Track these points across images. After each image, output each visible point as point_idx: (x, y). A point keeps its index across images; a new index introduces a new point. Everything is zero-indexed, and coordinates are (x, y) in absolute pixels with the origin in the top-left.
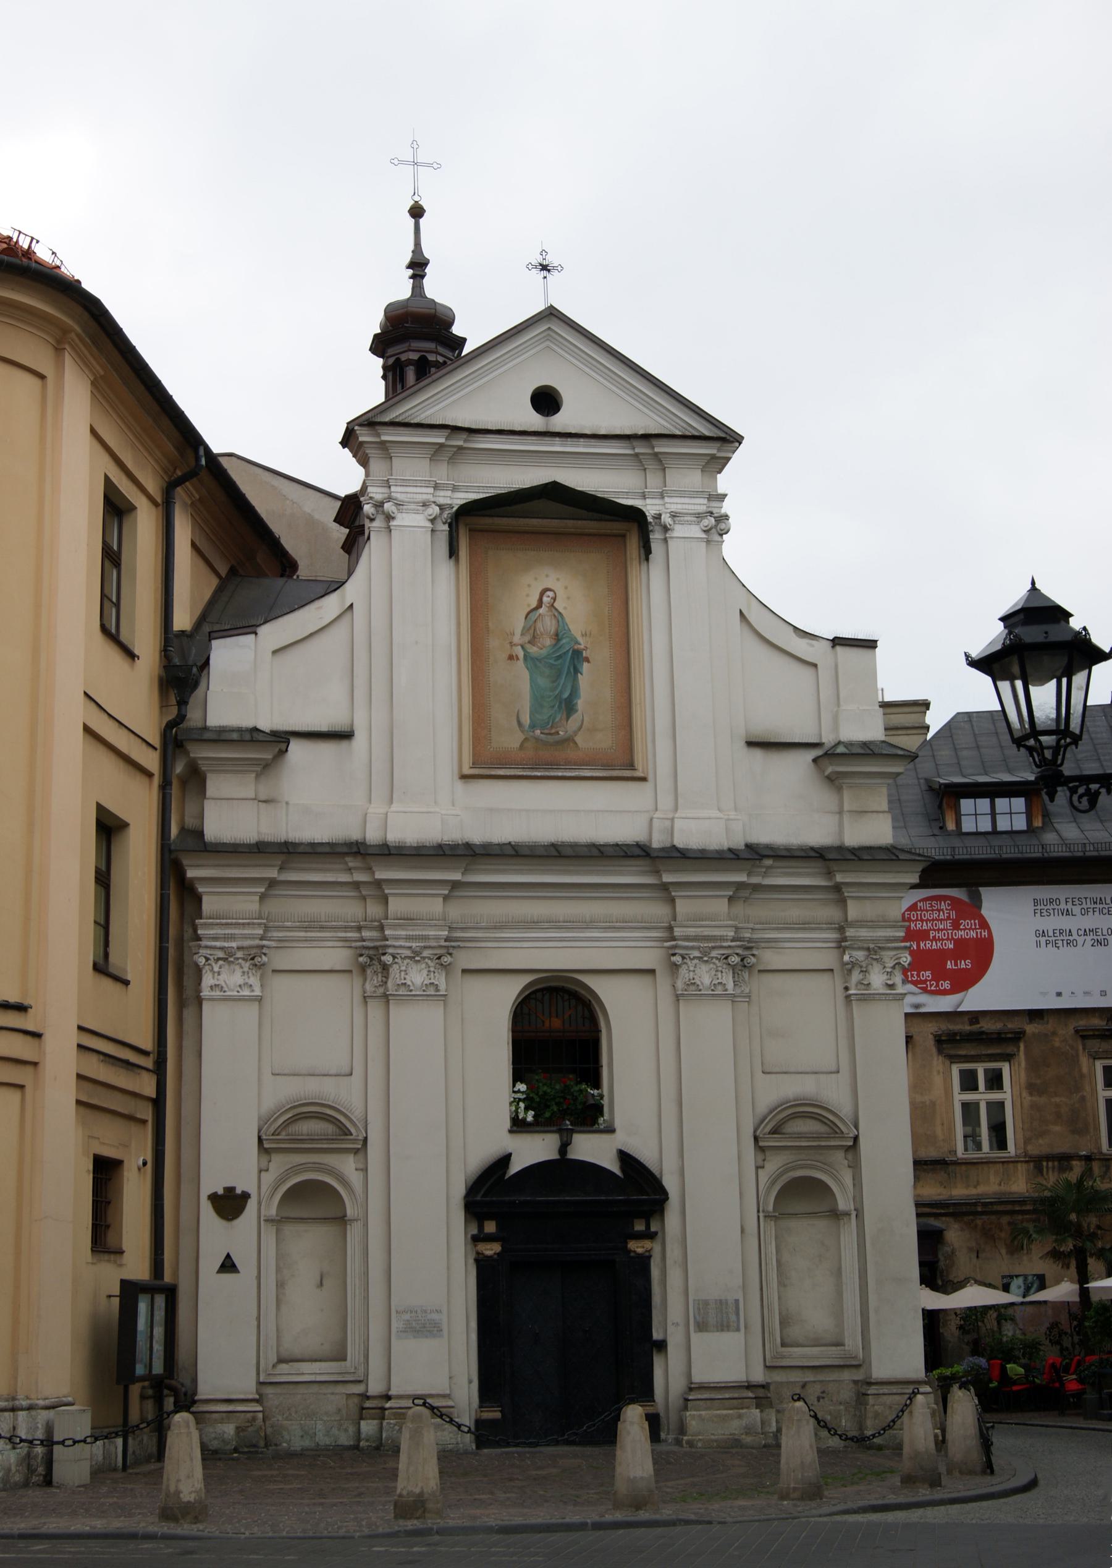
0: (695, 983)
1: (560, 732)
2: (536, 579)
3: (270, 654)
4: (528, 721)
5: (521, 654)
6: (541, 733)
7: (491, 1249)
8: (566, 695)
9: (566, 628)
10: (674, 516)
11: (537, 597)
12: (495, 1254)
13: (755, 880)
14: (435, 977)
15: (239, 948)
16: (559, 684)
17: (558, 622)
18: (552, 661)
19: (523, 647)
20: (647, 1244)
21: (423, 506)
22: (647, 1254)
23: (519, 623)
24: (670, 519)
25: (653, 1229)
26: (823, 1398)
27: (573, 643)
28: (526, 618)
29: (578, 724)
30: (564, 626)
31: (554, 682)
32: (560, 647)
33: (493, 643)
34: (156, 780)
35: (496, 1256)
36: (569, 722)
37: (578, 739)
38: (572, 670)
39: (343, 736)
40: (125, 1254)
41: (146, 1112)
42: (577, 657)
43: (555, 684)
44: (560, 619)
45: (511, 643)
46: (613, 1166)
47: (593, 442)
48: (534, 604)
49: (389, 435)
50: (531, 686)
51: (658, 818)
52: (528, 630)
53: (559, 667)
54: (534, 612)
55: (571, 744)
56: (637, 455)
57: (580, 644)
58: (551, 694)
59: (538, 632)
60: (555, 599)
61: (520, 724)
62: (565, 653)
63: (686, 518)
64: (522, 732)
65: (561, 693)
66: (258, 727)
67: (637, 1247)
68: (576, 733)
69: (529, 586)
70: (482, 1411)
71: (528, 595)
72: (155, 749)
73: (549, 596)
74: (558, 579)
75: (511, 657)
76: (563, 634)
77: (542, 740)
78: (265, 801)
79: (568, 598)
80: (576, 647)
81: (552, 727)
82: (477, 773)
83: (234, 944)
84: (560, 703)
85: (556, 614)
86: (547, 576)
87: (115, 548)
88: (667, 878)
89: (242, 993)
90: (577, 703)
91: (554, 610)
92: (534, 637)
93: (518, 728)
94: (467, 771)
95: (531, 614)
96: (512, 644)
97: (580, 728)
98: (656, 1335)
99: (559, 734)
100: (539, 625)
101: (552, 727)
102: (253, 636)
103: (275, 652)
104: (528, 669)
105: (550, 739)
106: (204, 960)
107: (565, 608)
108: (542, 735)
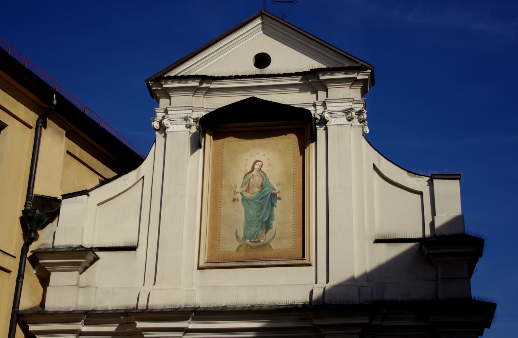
1: (261, 241)
2: (251, 156)
3: (96, 205)
4: (242, 235)
5: (240, 197)
6: (250, 242)
9: (268, 182)
10: (331, 113)
11: (251, 165)
13: (376, 323)
16: (262, 213)
17: (263, 178)
18: (258, 201)
19: (241, 193)
21: (185, 120)
23: (240, 180)
24: (328, 115)
27: (271, 190)
28: (244, 177)
29: (272, 236)
30: (266, 181)
31: (259, 212)
32: (264, 192)
33: (224, 192)
36: (267, 234)
37: (271, 244)
38: (270, 205)
39: (133, 248)
42: (274, 197)
43: (260, 213)
44: (264, 177)
45: (234, 192)
47: (284, 78)
48: (249, 169)
49: (167, 85)
50: (245, 215)
51: (317, 287)
52: (245, 184)
53: (263, 203)
54: (249, 174)
55: (268, 247)
56: (310, 84)
57: (275, 190)
58: (257, 219)
59: (251, 185)
60: (262, 166)
61: (237, 237)
62: (266, 196)
63: (338, 114)
64: (238, 241)
65: (263, 218)
66: (84, 246)
68: (271, 240)
69: (247, 160)
71: (246, 165)
72: (15, 257)
73: (258, 165)
74: (264, 155)
75: (234, 200)
76: (266, 185)
77: (250, 246)
78: (84, 287)
79: (270, 165)
80: (273, 192)
81: (256, 238)
82: (208, 266)
84: (262, 224)
85: (262, 174)
86: (258, 154)
90: (272, 224)
91: (261, 172)
92: (248, 188)
93: (236, 240)
94: (202, 264)
95: (247, 176)
96: (235, 193)
97: (273, 238)
99: (260, 242)
100: (252, 181)
101: (256, 238)
102: (86, 196)
103: (99, 205)
104: (244, 206)
105: (255, 245)
107: (268, 171)
108: (250, 243)
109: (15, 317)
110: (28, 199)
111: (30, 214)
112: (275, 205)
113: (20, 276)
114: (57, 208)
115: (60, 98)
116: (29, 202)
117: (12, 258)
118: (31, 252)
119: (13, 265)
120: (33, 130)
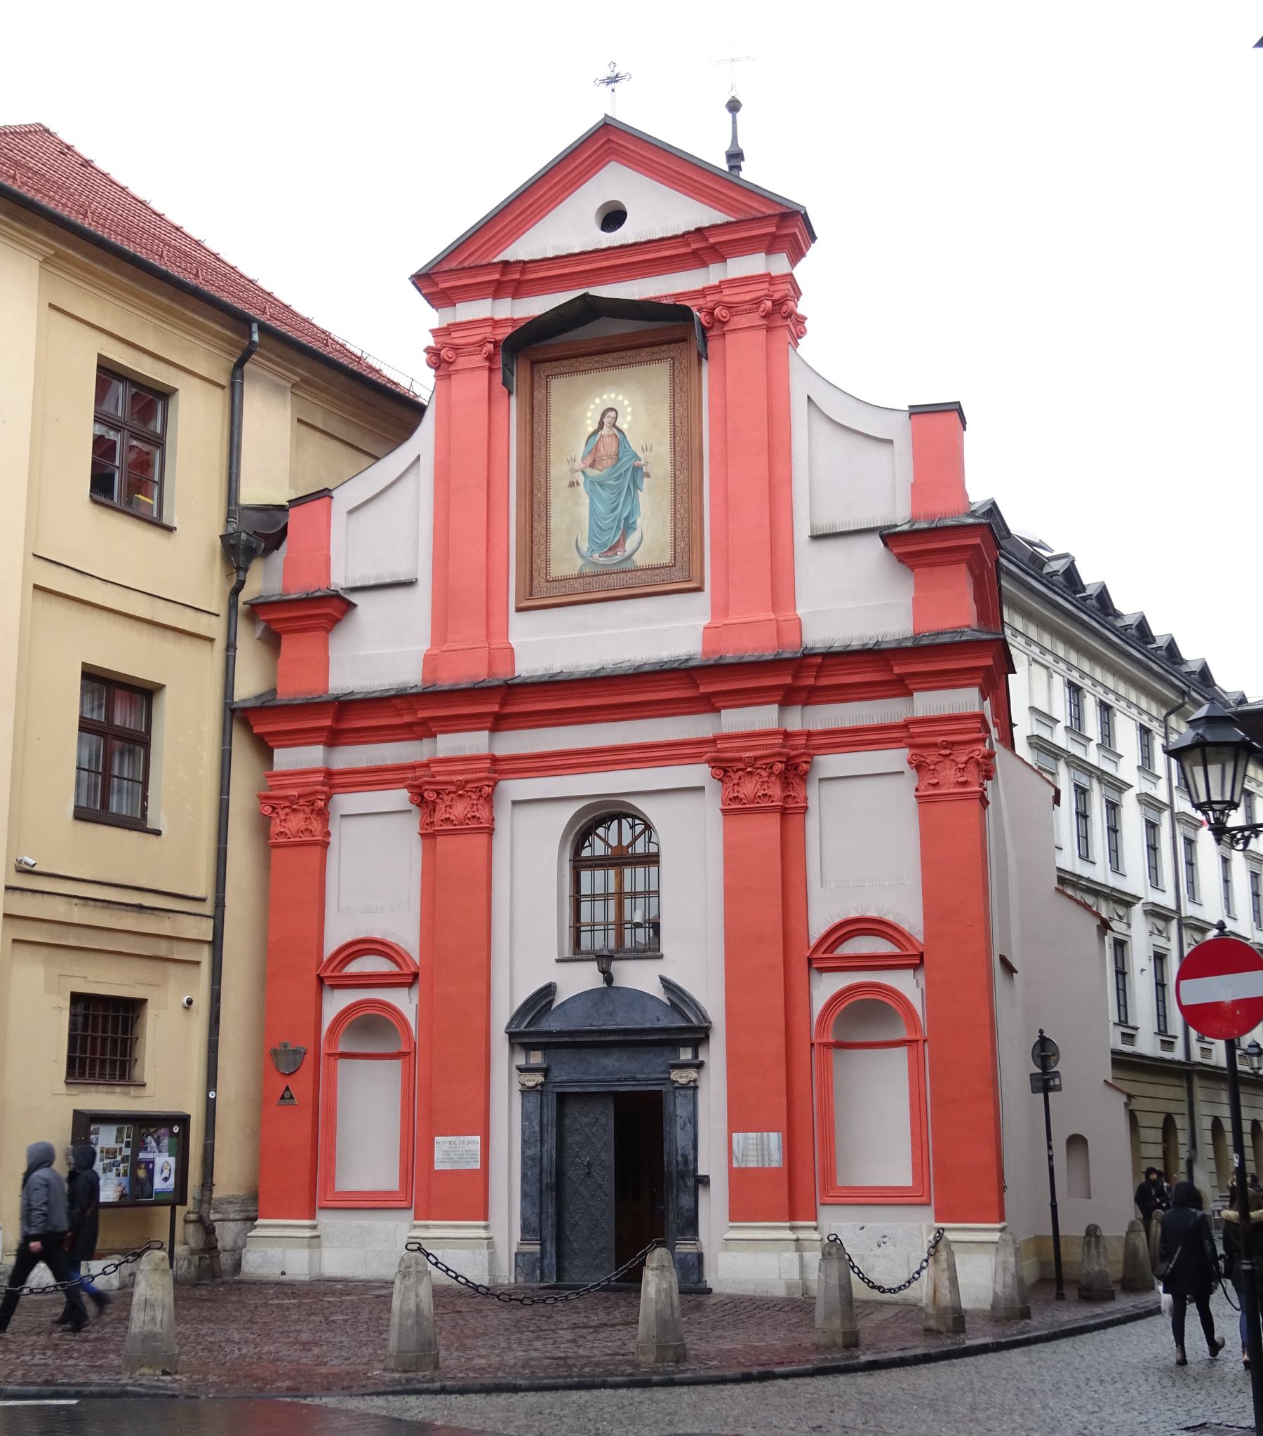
0: (738, 797)
3: (345, 514)
5: (581, 479)
7: (536, 1079)
8: (625, 515)
12: (537, 1085)
14: (477, 809)
15: (300, 796)
18: (611, 482)
19: (583, 472)
20: (693, 1074)
22: (692, 1084)
23: (580, 449)
25: (701, 1058)
26: (885, 1243)
34: (220, 644)
35: (539, 1088)
40: (147, 1087)
41: (205, 955)
42: (637, 473)
46: (656, 990)
48: (596, 426)
57: (640, 460)
67: (681, 1077)
70: (522, 1244)
75: (572, 485)
83: (295, 792)
87: (158, 431)
88: (703, 689)
89: (304, 839)
92: (594, 460)
98: (701, 1172)
103: (351, 512)
106: (270, 809)
108: (601, 559)
109: (229, 713)
110: (229, 514)
111: (232, 541)
112: (639, 486)
113: (231, 646)
114: (282, 525)
115: (263, 328)
116: (232, 520)
117: (214, 618)
118: (245, 603)
119: (216, 628)
120: (227, 390)
